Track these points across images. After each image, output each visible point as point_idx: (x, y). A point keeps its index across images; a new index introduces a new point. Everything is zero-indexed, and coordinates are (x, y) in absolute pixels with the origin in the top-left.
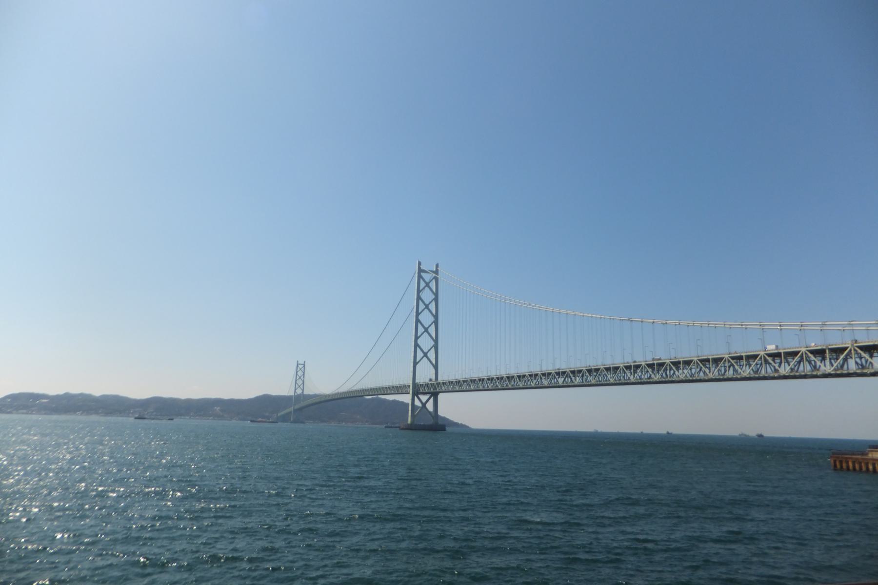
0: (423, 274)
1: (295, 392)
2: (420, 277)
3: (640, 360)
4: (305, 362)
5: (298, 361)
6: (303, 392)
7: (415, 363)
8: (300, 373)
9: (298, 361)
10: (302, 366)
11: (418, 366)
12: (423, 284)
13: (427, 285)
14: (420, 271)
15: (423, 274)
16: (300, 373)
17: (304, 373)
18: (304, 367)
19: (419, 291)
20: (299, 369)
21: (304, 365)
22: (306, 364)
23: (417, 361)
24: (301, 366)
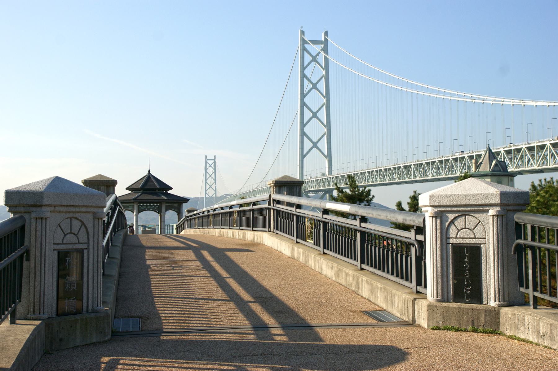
0: (306, 45)
1: (206, 193)
2: (304, 50)
3: (357, 170)
4: (215, 156)
5: (206, 156)
6: (216, 193)
7: (303, 156)
8: (211, 171)
9: (206, 156)
10: (214, 161)
11: (305, 159)
12: (308, 58)
13: (314, 59)
14: (304, 42)
15: (306, 45)
16: (211, 171)
17: (215, 169)
18: (215, 162)
19: (303, 68)
20: (208, 165)
21: (214, 160)
22: (216, 160)
23: (305, 153)
24: (210, 162)
